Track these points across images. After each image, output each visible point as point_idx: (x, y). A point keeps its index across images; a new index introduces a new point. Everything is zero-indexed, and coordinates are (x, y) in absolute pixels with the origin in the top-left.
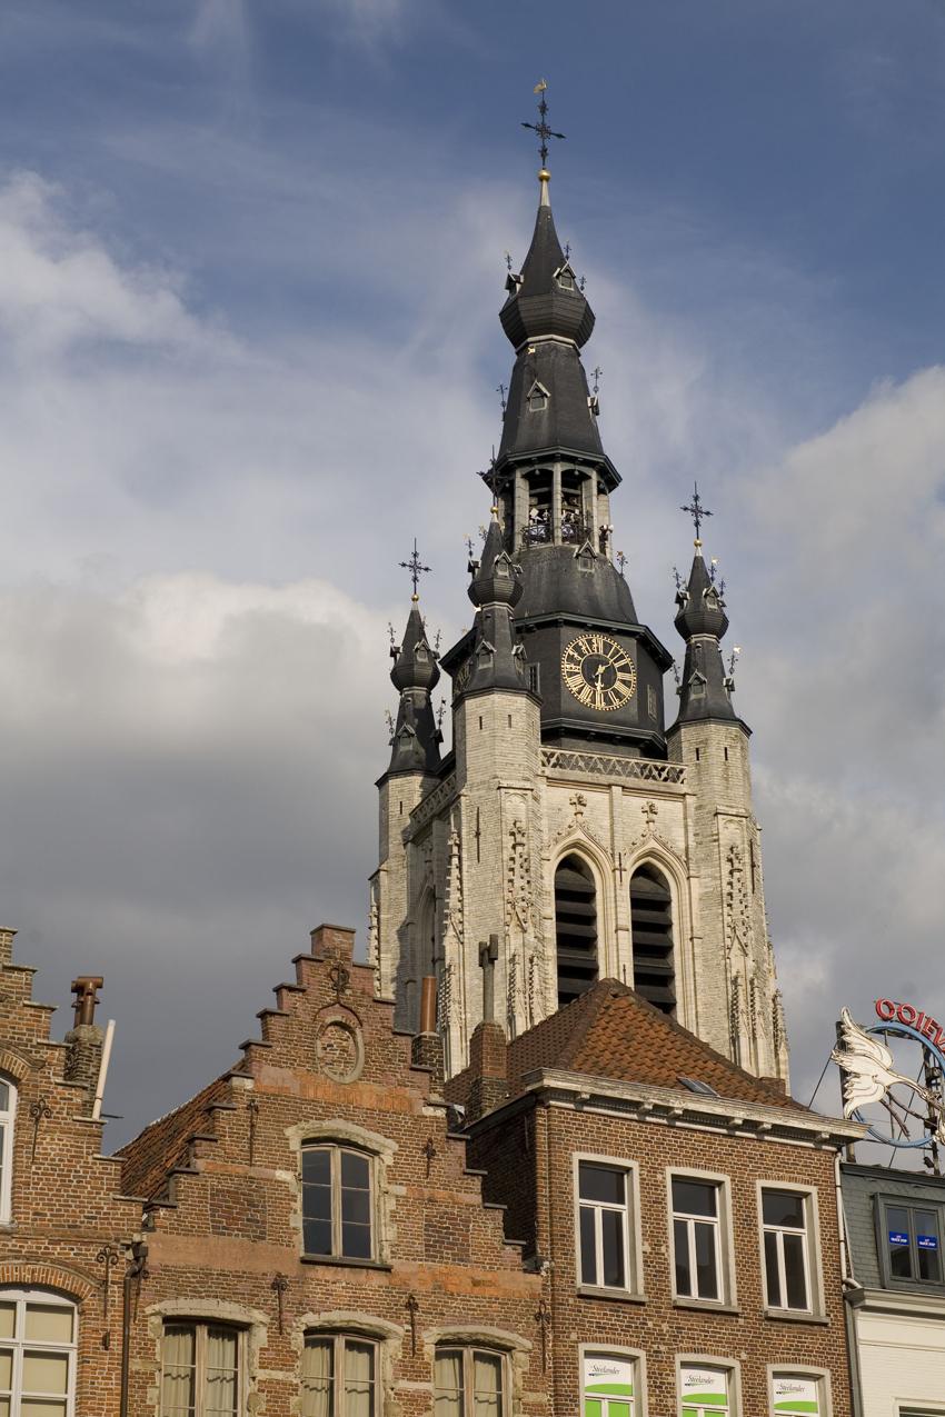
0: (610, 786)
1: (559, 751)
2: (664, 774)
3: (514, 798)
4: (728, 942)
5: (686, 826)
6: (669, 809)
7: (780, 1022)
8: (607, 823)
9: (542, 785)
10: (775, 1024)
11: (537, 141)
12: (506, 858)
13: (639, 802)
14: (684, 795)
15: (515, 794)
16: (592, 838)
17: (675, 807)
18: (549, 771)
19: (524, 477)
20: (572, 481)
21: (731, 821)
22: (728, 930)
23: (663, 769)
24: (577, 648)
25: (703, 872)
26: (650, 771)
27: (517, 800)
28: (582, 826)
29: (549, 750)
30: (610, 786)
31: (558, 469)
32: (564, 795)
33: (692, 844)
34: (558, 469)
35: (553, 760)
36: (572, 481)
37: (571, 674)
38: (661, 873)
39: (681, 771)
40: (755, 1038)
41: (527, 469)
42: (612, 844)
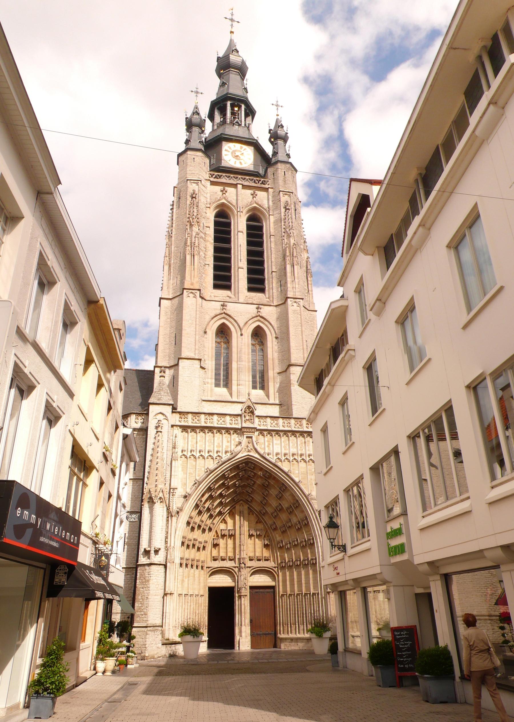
0: (236, 185)
1: (216, 173)
2: (260, 182)
3: (193, 184)
4: (283, 234)
5: (268, 200)
6: (261, 195)
7: (309, 267)
8: (235, 198)
9: (209, 183)
10: (307, 268)
11: (230, 23)
12: (188, 202)
13: (249, 192)
14: (268, 189)
15: (194, 183)
16: (229, 202)
17: (264, 194)
18: (212, 179)
19: (218, 109)
21: (286, 194)
22: (283, 230)
23: (260, 181)
24: (229, 147)
25: (275, 213)
26: (255, 181)
27: (194, 185)
28: (225, 198)
29: (212, 173)
30: (236, 185)
31: (229, 103)
32: (218, 188)
33: (271, 203)
34: (229, 103)
35: (214, 176)
37: (226, 155)
38: (260, 218)
39: (268, 181)
40: (293, 266)
41: (218, 106)
42: (237, 203)
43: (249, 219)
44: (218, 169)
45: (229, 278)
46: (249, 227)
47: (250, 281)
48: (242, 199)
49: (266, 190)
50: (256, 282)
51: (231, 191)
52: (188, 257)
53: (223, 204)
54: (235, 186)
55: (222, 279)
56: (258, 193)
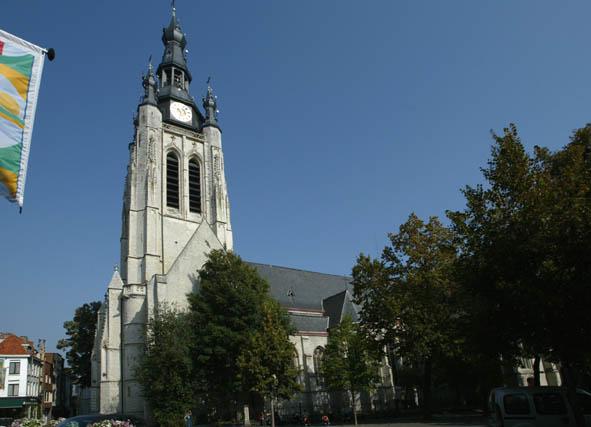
6: (199, 145)
13: (191, 142)
20: (178, 73)
34: (173, 68)
36: (178, 73)
43: (190, 161)
44: (168, 120)
45: (177, 201)
46: (190, 167)
47: (191, 204)
48: (187, 147)
49: (203, 143)
50: (196, 206)
51: (178, 140)
52: (149, 183)
53: (173, 148)
54: (181, 136)
55: (173, 200)
56: (198, 144)
